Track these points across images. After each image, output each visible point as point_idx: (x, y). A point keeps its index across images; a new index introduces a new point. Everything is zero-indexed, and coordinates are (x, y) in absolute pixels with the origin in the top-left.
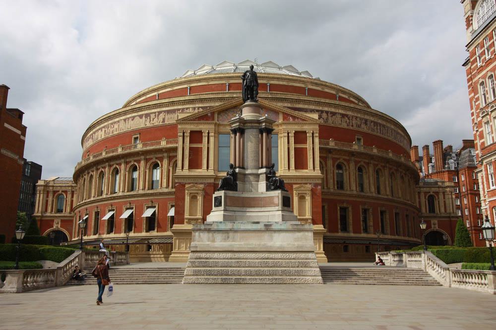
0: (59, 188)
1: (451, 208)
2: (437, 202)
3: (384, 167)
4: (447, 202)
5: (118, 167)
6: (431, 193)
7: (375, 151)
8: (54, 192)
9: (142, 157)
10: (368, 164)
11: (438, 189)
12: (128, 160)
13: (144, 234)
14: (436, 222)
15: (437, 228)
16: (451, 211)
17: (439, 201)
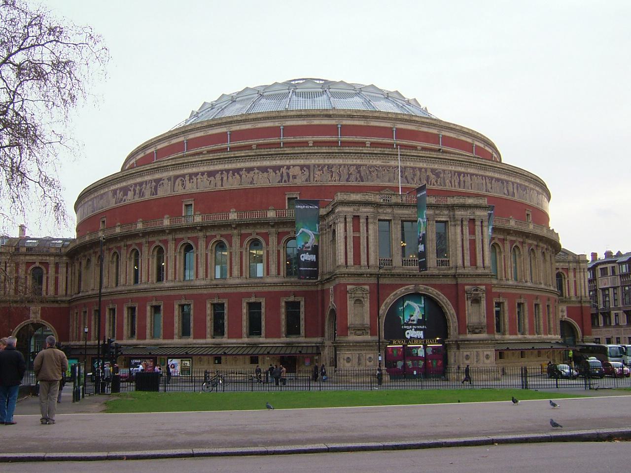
0: (34, 258)
1: (583, 292)
2: (566, 283)
3: (537, 246)
4: (578, 282)
5: (190, 242)
6: (560, 270)
7: (531, 227)
8: (28, 264)
9: (235, 232)
10: (522, 243)
11: (567, 264)
12: (208, 234)
13: (246, 340)
14: (565, 308)
15: (566, 317)
16: (583, 294)
17: (568, 281)
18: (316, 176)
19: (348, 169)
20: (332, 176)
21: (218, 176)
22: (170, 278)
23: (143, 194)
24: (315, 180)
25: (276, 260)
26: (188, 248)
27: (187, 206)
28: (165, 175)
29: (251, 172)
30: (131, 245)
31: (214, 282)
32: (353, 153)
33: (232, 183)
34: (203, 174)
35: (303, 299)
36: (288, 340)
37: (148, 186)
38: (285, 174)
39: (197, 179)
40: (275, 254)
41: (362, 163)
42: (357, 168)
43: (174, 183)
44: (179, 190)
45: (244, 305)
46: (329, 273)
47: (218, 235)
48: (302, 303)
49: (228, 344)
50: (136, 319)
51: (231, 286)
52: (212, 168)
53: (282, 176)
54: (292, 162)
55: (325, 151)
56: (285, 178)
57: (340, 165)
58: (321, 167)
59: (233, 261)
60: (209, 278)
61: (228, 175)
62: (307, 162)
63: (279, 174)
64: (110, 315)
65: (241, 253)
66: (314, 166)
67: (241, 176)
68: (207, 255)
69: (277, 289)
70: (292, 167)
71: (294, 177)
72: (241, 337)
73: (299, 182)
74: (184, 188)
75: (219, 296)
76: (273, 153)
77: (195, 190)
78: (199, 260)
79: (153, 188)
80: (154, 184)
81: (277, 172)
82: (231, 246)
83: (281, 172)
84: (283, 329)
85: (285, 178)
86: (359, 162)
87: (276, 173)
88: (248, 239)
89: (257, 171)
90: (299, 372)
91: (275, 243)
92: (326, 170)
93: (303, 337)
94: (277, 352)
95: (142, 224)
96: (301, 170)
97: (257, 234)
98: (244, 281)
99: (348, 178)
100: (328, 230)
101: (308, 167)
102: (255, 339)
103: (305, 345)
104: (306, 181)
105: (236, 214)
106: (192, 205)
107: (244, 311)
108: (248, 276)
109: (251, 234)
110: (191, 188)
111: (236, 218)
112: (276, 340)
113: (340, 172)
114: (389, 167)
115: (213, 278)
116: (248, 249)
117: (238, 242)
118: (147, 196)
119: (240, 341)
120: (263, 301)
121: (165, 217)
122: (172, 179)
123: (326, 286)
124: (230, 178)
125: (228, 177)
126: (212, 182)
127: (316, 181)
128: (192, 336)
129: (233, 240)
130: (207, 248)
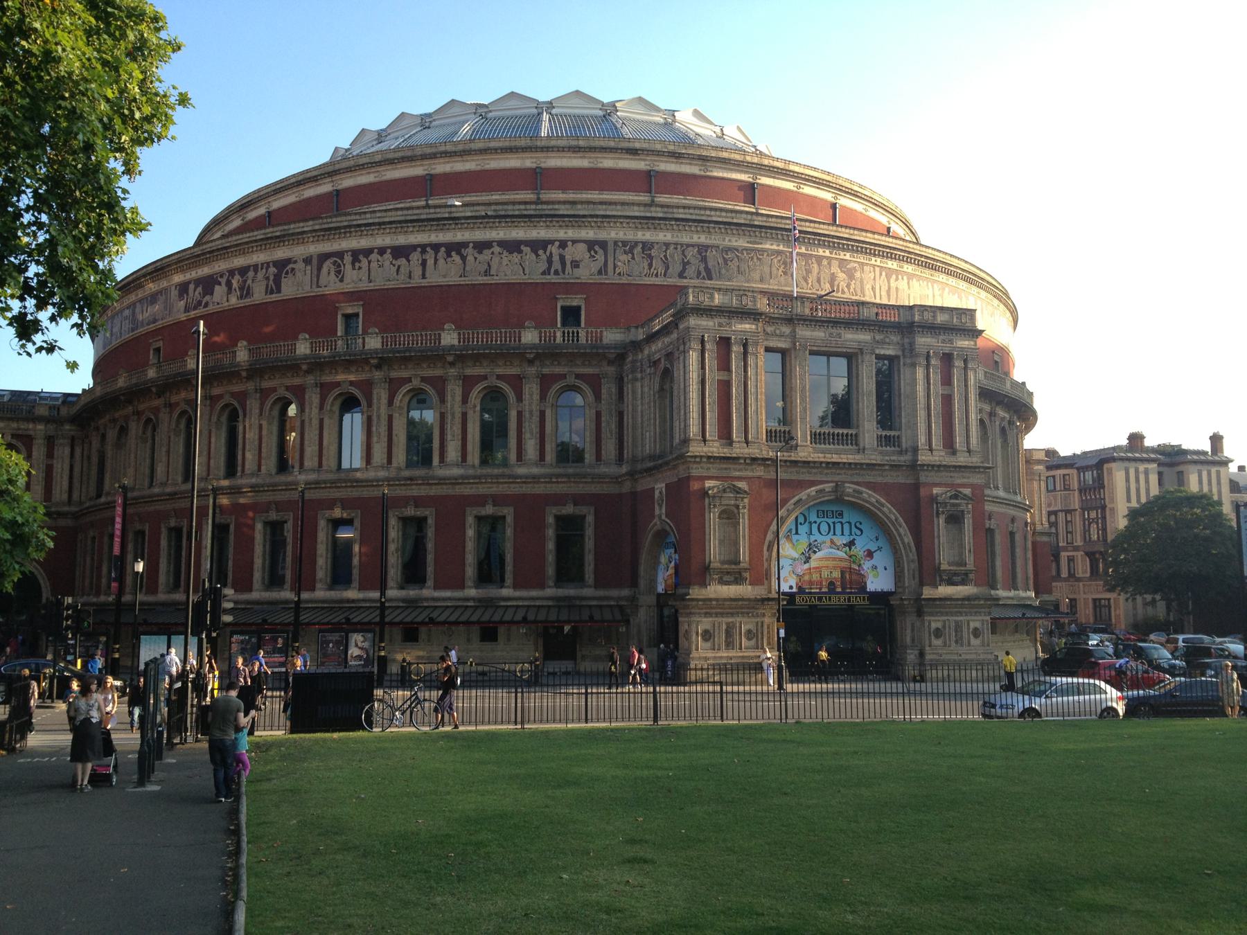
9: (452, 371)
12: (394, 374)
13: (472, 592)
20: (650, 265)
21: (415, 257)
22: (308, 464)
23: (248, 293)
24: (618, 271)
25: (536, 430)
26: (349, 404)
27: (348, 317)
28: (297, 251)
29: (486, 252)
30: (220, 397)
31: (407, 473)
32: (694, 221)
33: (445, 273)
34: (382, 251)
35: (592, 510)
36: (561, 592)
37: (260, 275)
38: (556, 258)
39: (369, 262)
40: (536, 419)
41: (709, 242)
42: (700, 253)
43: (319, 269)
44: (330, 285)
45: (470, 520)
46: (652, 457)
47: (415, 375)
48: (590, 519)
49: (434, 599)
50: (231, 550)
51: (442, 481)
52: (402, 240)
53: (550, 261)
54: (571, 234)
55: (637, 214)
56: (557, 265)
57: (667, 245)
58: (629, 247)
59: (449, 432)
60: (395, 464)
61: (436, 254)
62: (602, 235)
63: (544, 257)
64: (169, 541)
65: (464, 415)
66: (616, 243)
67: (464, 258)
68: (390, 418)
69: (539, 489)
70: (570, 243)
71: (576, 264)
72: (462, 586)
73: (586, 273)
74: (341, 281)
75: (418, 502)
76: (532, 212)
77: (364, 286)
78: (374, 429)
79: (272, 278)
80: (273, 270)
81: (541, 252)
82: (443, 400)
84: (551, 571)
85: (557, 265)
86: (702, 239)
87: (537, 255)
88: (479, 387)
89: (497, 249)
90: (583, 657)
91: (536, 397)
93: (590, 586)
94: (541, 617)
95: (246, 352)
96: (589, 251)
97: (499, 377)
98: (471, 472)
99: (684, 270)
100: (648, 371)
101: (603, 244)
102: (492, 592)
103: (594, 603)
104: (600, 272)
105: (455, 335)
106: (357, 315)
107: (470, 533)
108: (477, 462)
109: (485, 378)
110: (354, 279)
111: (456, 342)
112: (534, 593)
114: (763, 250)
115: (403, 465)
116: (478, 408)
117: (458, 392)
118: (259, 295)
119: (458, 594)
120: (508, 512)
121: (300, 337)
122: (315, 261)
123: (643, 484)
124: (441, 262)
125: (436, 260)
126: (402, 270)
128: (355, 584)
129: (449, 388)
130: (390, 403)
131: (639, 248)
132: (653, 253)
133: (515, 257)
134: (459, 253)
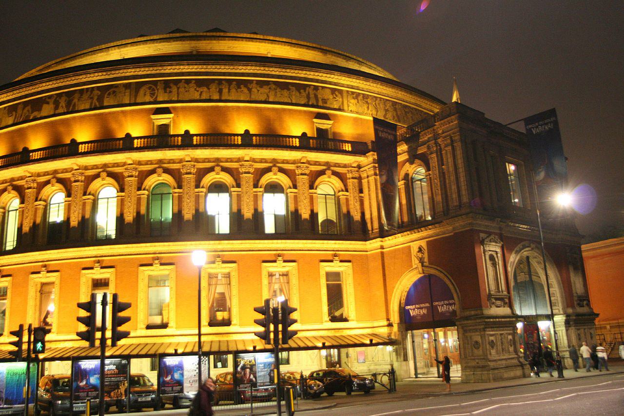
18: (350, 104)
19: (385, 104)
20: (368, 108)
21: (213, 87)
29: (265, 87)
34: (188, 82)
37: (85, 96)
39: (178, 88)
53: (308, 97)
61: (230, 86)
67: (250, 90)
79: (96, 98)
81: (302, 91)
83: (307, 92)
92: (361, 100)
96: (332, 94)
113: (376, 105)
127: (351, 111)
131: (361, 97)
132: (369, 101)
133: (285, 92)
134: (246, 86)
